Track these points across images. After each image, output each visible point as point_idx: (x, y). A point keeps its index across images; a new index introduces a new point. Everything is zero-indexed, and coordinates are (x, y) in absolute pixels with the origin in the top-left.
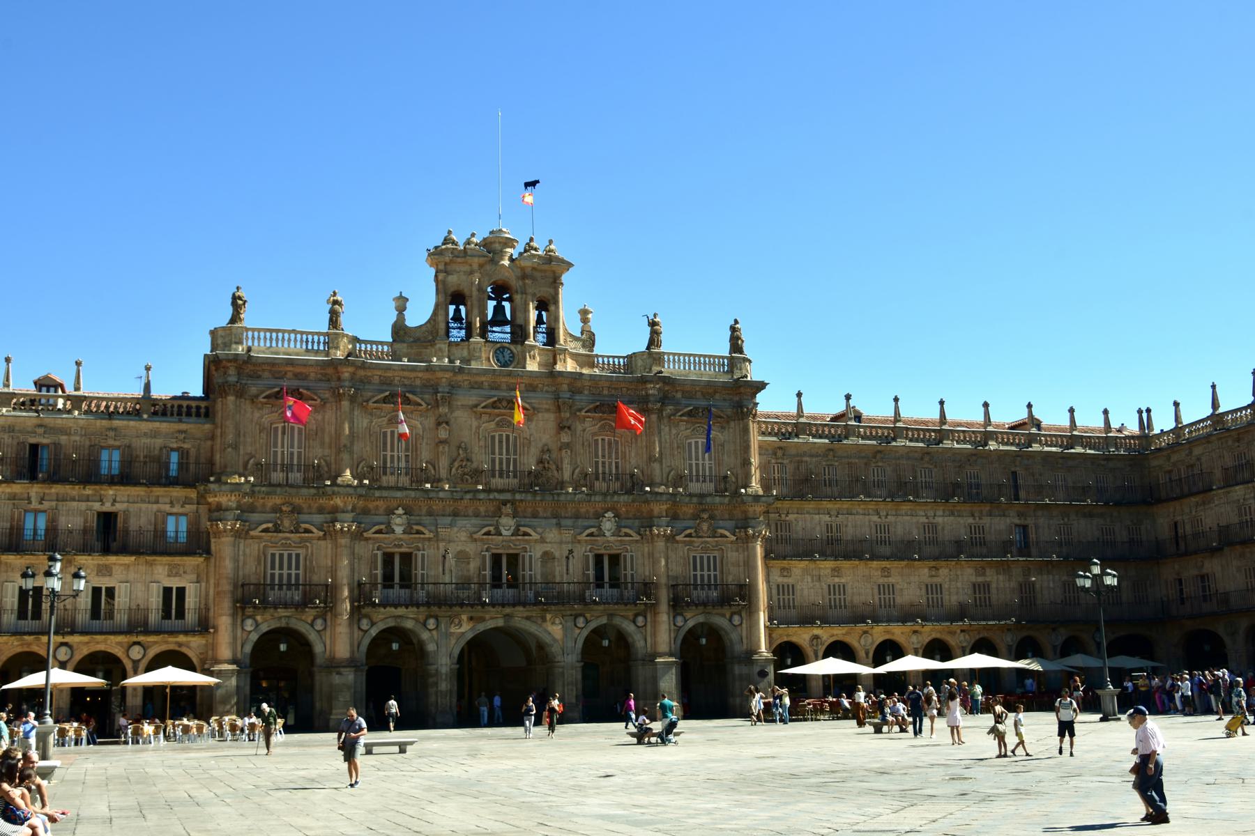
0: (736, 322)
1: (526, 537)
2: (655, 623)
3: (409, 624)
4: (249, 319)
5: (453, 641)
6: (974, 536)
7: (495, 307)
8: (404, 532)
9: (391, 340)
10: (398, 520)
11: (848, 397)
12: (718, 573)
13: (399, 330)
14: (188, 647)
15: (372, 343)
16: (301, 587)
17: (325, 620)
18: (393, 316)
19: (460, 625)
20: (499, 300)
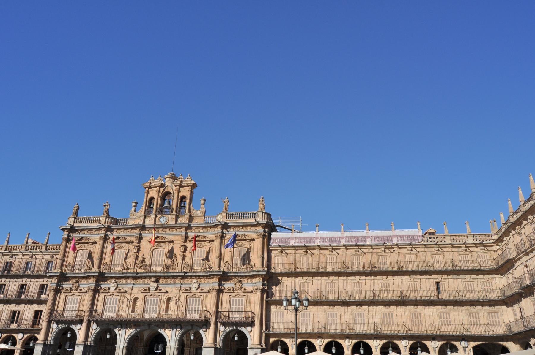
1: (160, 291)
3: (111, 327)
6: (383, 288)
8: (115, 289)
10: (113, 285)
12: (243, 307)
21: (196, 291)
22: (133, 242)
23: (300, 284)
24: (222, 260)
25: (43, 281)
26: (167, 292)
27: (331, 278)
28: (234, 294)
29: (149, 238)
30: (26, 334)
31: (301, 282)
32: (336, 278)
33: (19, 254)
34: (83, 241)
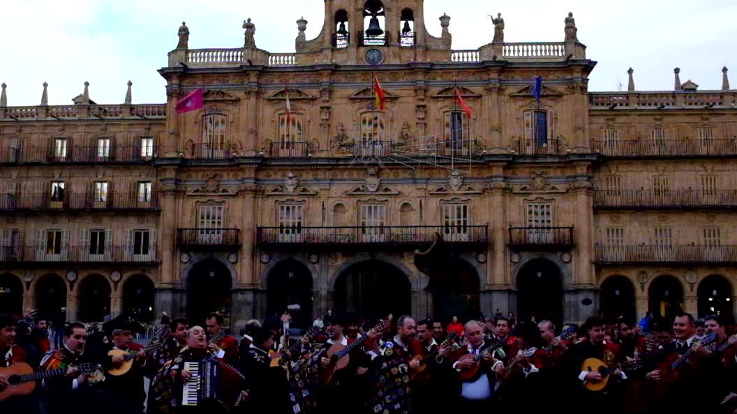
0: (571, 15)
2: (493, 258)
3: (298, 258)
4: (192, 45)
5: (331, 272)
7: (371, 21)
9: (295, 52)
10: (289, 182)
11: (677, 71)
13: (301, 43)
14: (150, 273)
15: (280, 55)
16: (221, 231)
17: (237, 256)
18: (296, 33)
19: (336, 258)
20: (374, 14)
21: (460, 192)
22: (313, 99)
23: (650, 177)
24: (503, 134)
25: (138, 174)
26: (399, 194)
27: (709, 167)
28: (533, 197)
29: (352, 91)
30: (125, 272)
31: (654, 174)
32: (718, 167)
33: (79, 124)
34: (211, 99)
